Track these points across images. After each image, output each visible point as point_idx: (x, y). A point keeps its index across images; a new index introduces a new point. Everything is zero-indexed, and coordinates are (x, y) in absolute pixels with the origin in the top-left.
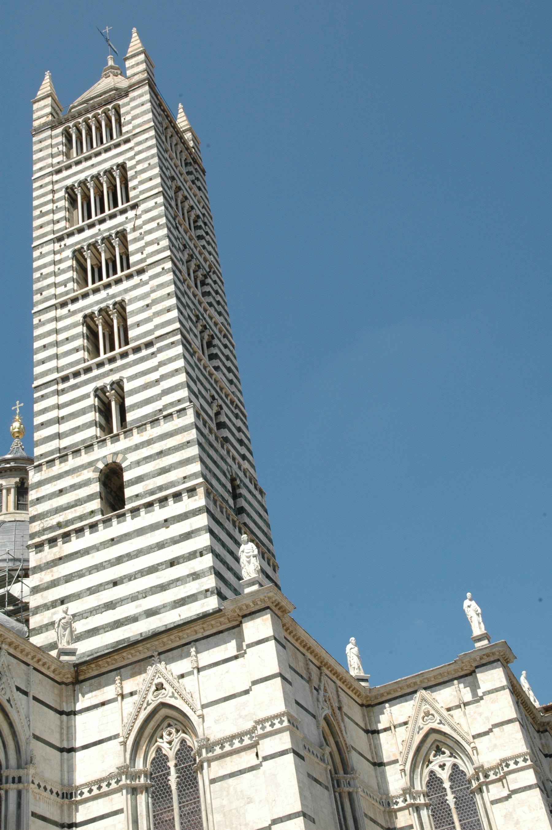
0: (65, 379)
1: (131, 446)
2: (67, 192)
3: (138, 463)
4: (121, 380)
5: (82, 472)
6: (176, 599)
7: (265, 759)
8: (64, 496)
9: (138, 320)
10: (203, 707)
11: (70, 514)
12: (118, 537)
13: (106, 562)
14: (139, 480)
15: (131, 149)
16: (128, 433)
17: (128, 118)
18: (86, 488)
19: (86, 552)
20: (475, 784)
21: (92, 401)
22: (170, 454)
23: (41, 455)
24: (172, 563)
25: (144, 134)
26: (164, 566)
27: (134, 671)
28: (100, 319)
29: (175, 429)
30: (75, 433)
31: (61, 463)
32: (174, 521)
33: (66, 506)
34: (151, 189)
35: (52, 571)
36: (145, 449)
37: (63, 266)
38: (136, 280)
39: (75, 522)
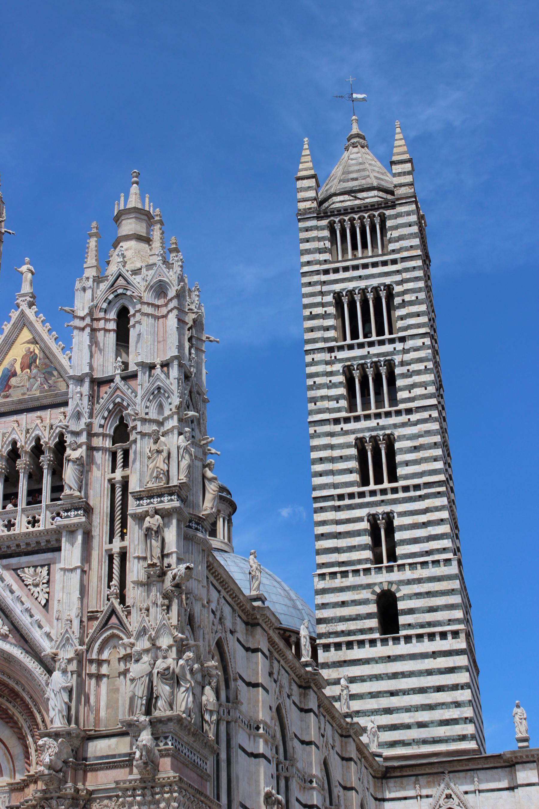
0: (341, 497)
1: (404, 580)
2: (334, 298)
3: (410, 597)
4: (392, 512)
6: (441, 719)
8: (346, 608)
9: (407, 459)
12: (394, 656)
13: (384, 674)
14: (411, 611)
15: (398, 272)
16: (401, 567)
17: (395, 234)
18: (365, 606)
19: (367, 661)
21: (365, 525)
22: (437, 596)
23: (323, 564)
24: (439, 689)
25: (412, 261)
26: (432, 690)
27: (429, 780)
28: (370, 445)
29: (442, 576)
30: (351, 551)
31: (342, 577)
32: (440, 654)
33: (348, 617)
34: (418, 326)
35: (338, 671)
36: (415, 586)
38: (404, 418)
39: (356, 633)
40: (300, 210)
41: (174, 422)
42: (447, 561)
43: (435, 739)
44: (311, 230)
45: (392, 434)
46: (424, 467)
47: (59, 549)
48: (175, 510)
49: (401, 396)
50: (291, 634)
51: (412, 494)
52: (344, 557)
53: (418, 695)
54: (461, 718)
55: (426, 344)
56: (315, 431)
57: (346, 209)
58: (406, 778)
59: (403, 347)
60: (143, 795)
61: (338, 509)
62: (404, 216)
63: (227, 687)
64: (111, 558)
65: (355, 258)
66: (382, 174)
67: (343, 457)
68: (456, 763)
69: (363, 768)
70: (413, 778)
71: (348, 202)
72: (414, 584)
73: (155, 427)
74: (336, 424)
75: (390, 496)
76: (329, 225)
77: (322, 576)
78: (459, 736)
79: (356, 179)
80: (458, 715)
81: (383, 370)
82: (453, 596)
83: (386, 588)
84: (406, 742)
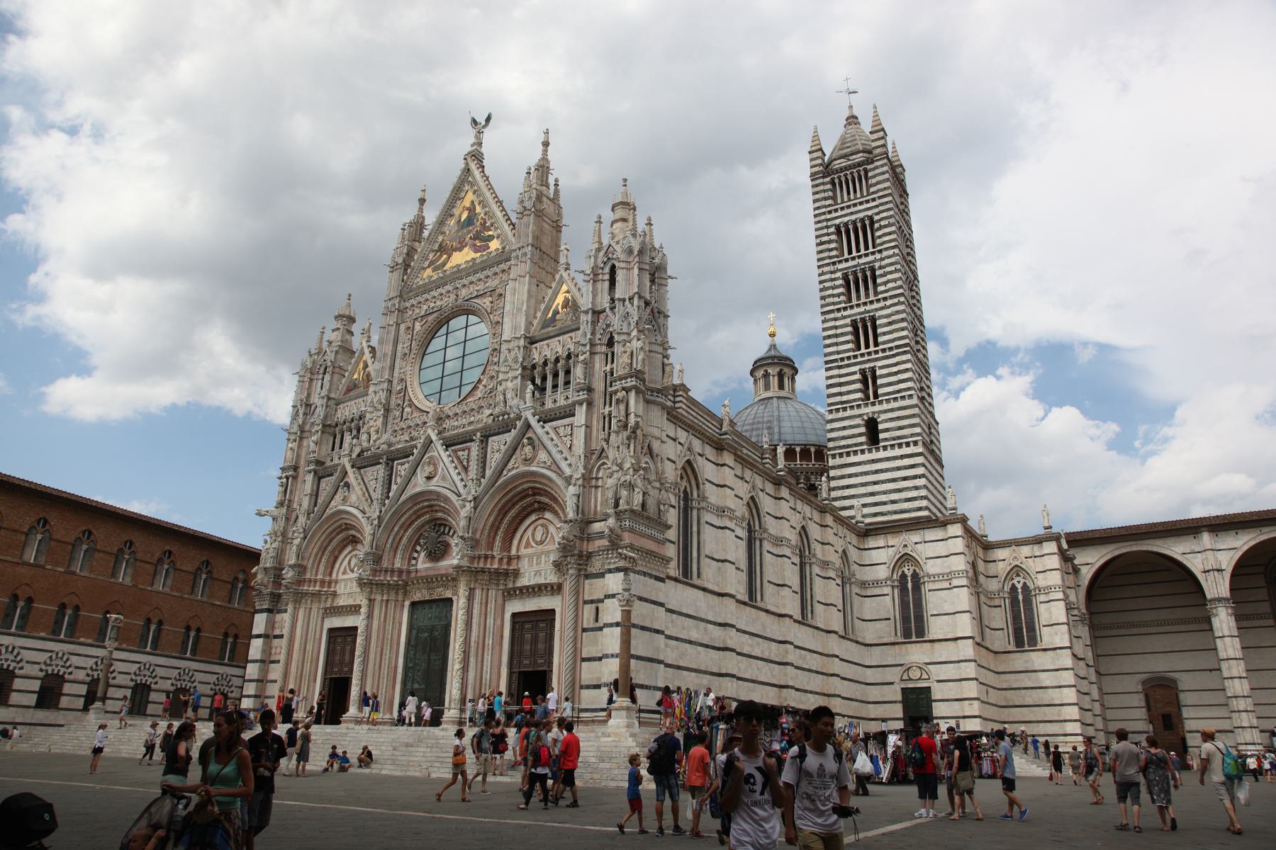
0: (842, 359)
4: (875, 366)
7: (955, 587)
10: (926, 559)
11: (850, 442)
14: (887, 430)
15: (877, 206)
17: (874, 181)
20: (1033, 593)
21: (858, 376)
24: (905, 479)
38: (882, 304)
41: (634, 333)
45: (874, 315)
47: (574, 415)
48: (635, 387)
51: (888, 353)
52: (845, 398)
57: (841, 169)
60: (612, 554)
61: (840, 367)
63: (698, 488)
64: (602, 417)
65: (849, 200)
69: (846, 531)
71: (842, 163)
73: (625, 337)
75: (874, 356)
77: (831, 412)
79: (848, 147)
81: (868, 273)
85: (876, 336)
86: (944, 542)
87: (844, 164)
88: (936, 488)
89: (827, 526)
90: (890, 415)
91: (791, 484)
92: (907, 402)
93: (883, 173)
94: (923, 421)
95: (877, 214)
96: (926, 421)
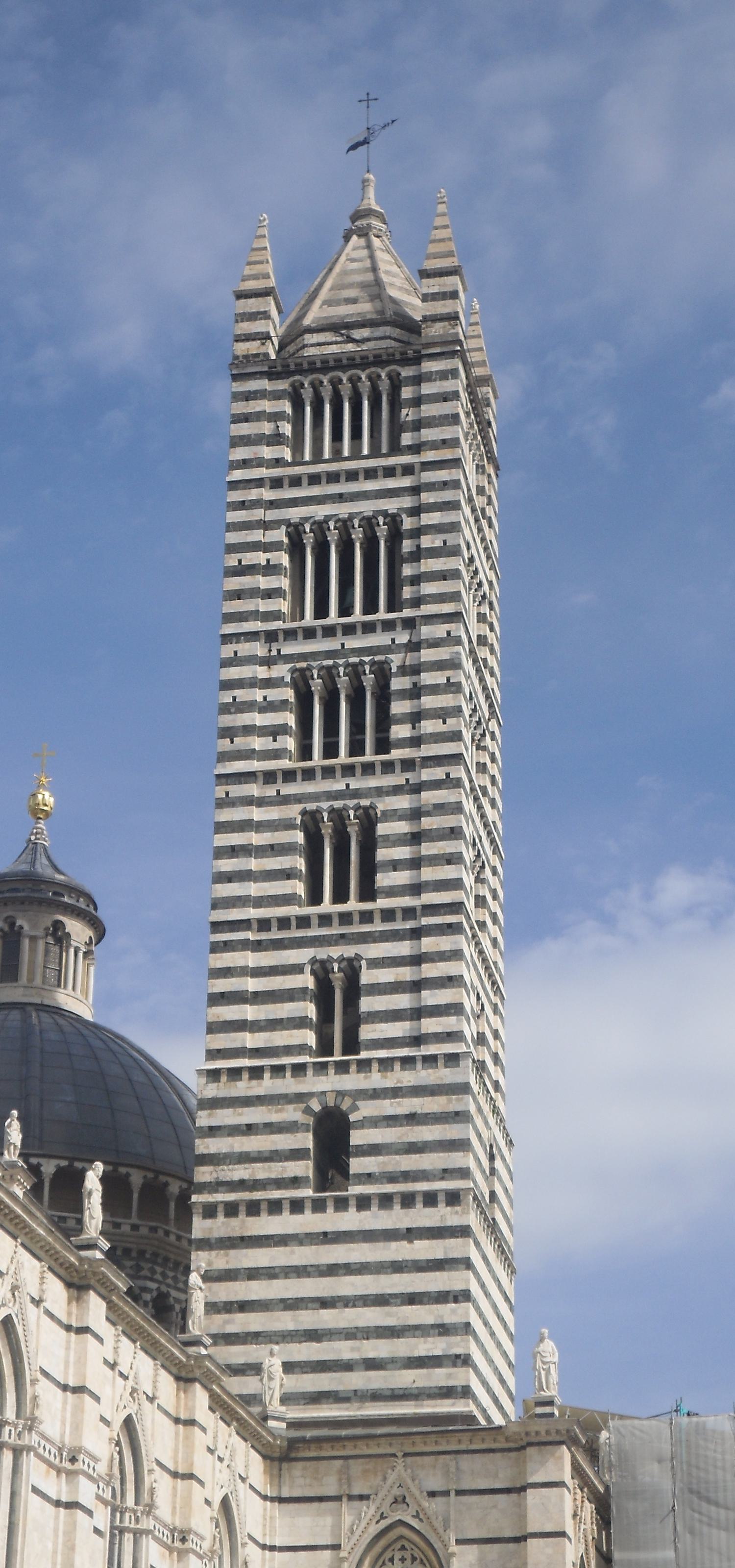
0: (264, 925)
1: (367, 1090)
2: (288, 535)
4: (358, 957)
5: (286, 1107)
11: (261, 1171)
13: (312, 1266)
14: (374, 1150)
18: (289, 1135)
19: (282, 1240)
23: (219, 1051)
24: (412, 1299)
26: (399, 1301)
29: (438, 1085)
31: (251, 1078)
33: (256, 1155)
35: (227, 1255)
36: (387, 1102)
37: (274, 695)
40: (236, 357)
42: (453, 1059)
43: (396, 1393)
44: (255, 399)
45: (373, 807)
46: (428, 874)
49: (397, 733)
50: (170, 1180)
51: (399, 925)
53: (373, 1308)
54: (448, 1357)
55: (452, 634)
56: (227, 794)
57: (325, 362)
58: (325, 1462)
59: (408, 638)
61: (258, 946)
62: (435, 380)
66: (408, 292)
67: (276, 847)
68: (418, 1439)
70: (338, 1463)
72: (384, 1099)
74: (268, 783)
75: (358, 928)
76: (290, 390)
77: (214, 1075)
78: (441, 1388)
80: (443, 1350)
81: (369, 680)
82: (455, 1125)
83: (331, 1104)
84: (341, 1395)
85: (369, 869)
86: (514, 1496)
87: (334, 349)
88: (493, 1334)
89: (191, 1422)
90: (388, 1107)
91: (114, 1289)
92: (443, 1075)
93: (445, 397)
94: (479, 1136)
95: (415, 512)
96: (485, 1134)
